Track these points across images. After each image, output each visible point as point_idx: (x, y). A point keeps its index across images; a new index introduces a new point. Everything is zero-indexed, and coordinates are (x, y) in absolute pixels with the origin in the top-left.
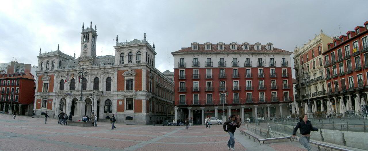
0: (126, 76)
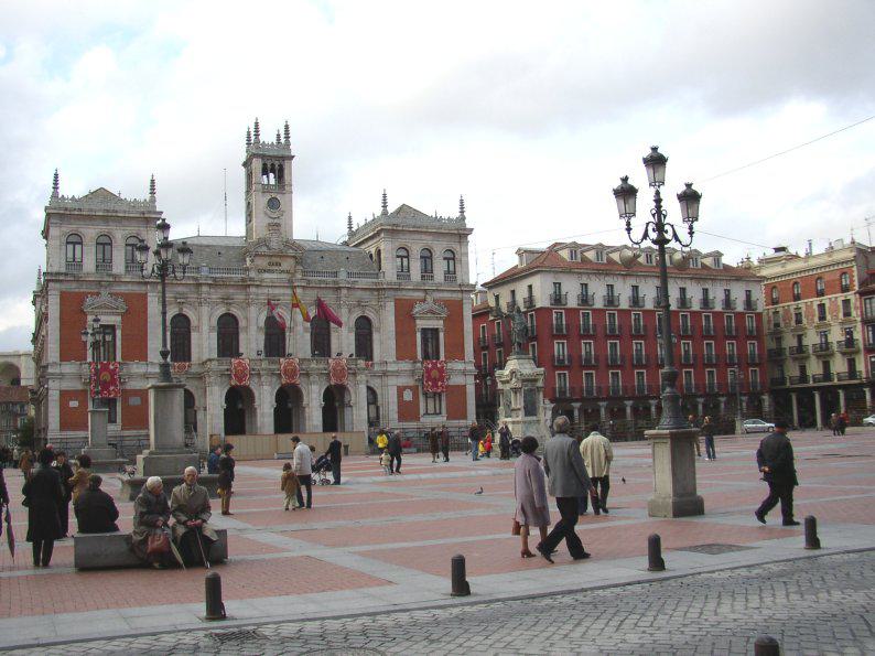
0: (421, 318)
